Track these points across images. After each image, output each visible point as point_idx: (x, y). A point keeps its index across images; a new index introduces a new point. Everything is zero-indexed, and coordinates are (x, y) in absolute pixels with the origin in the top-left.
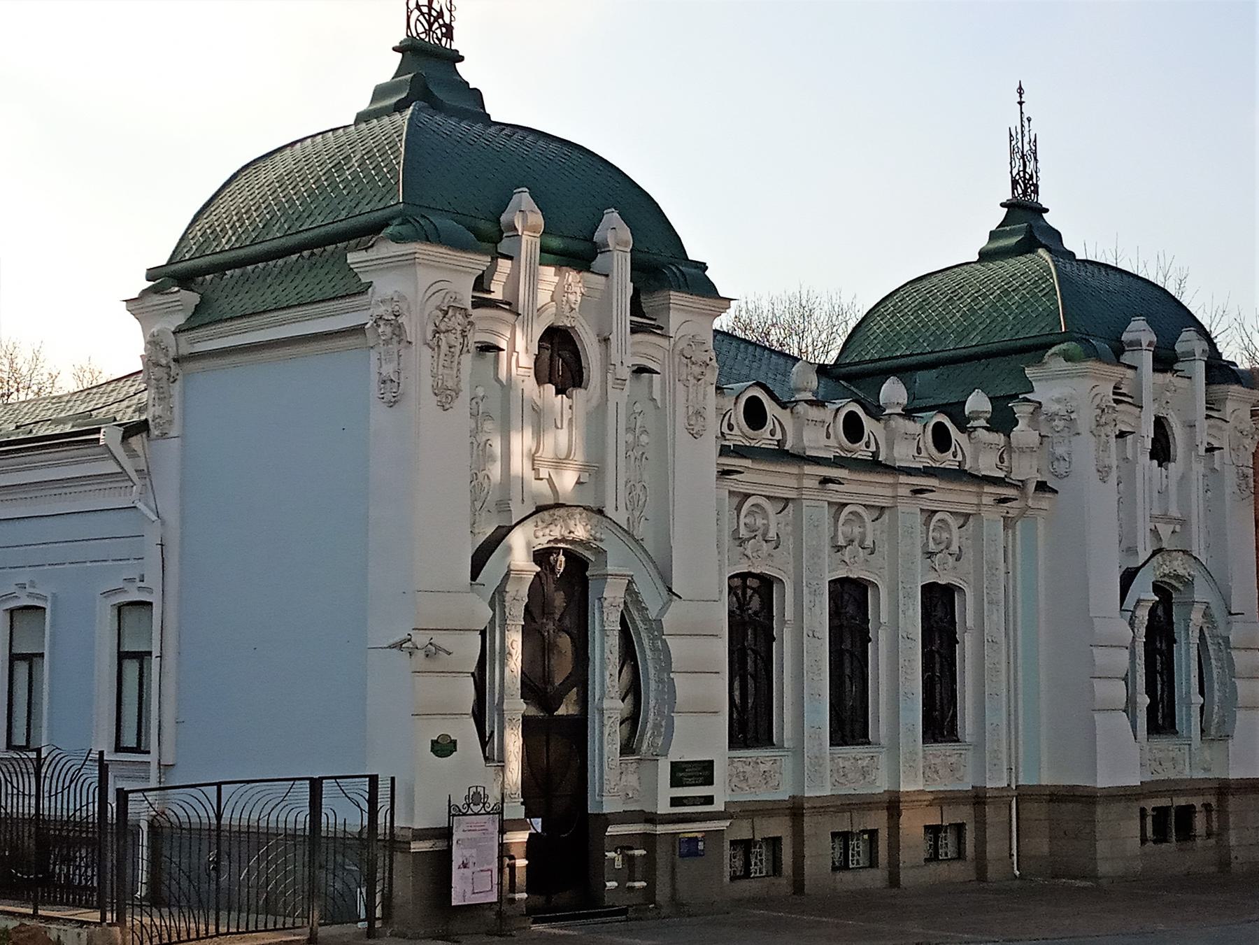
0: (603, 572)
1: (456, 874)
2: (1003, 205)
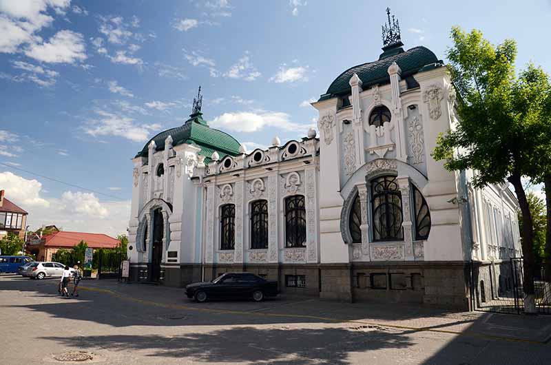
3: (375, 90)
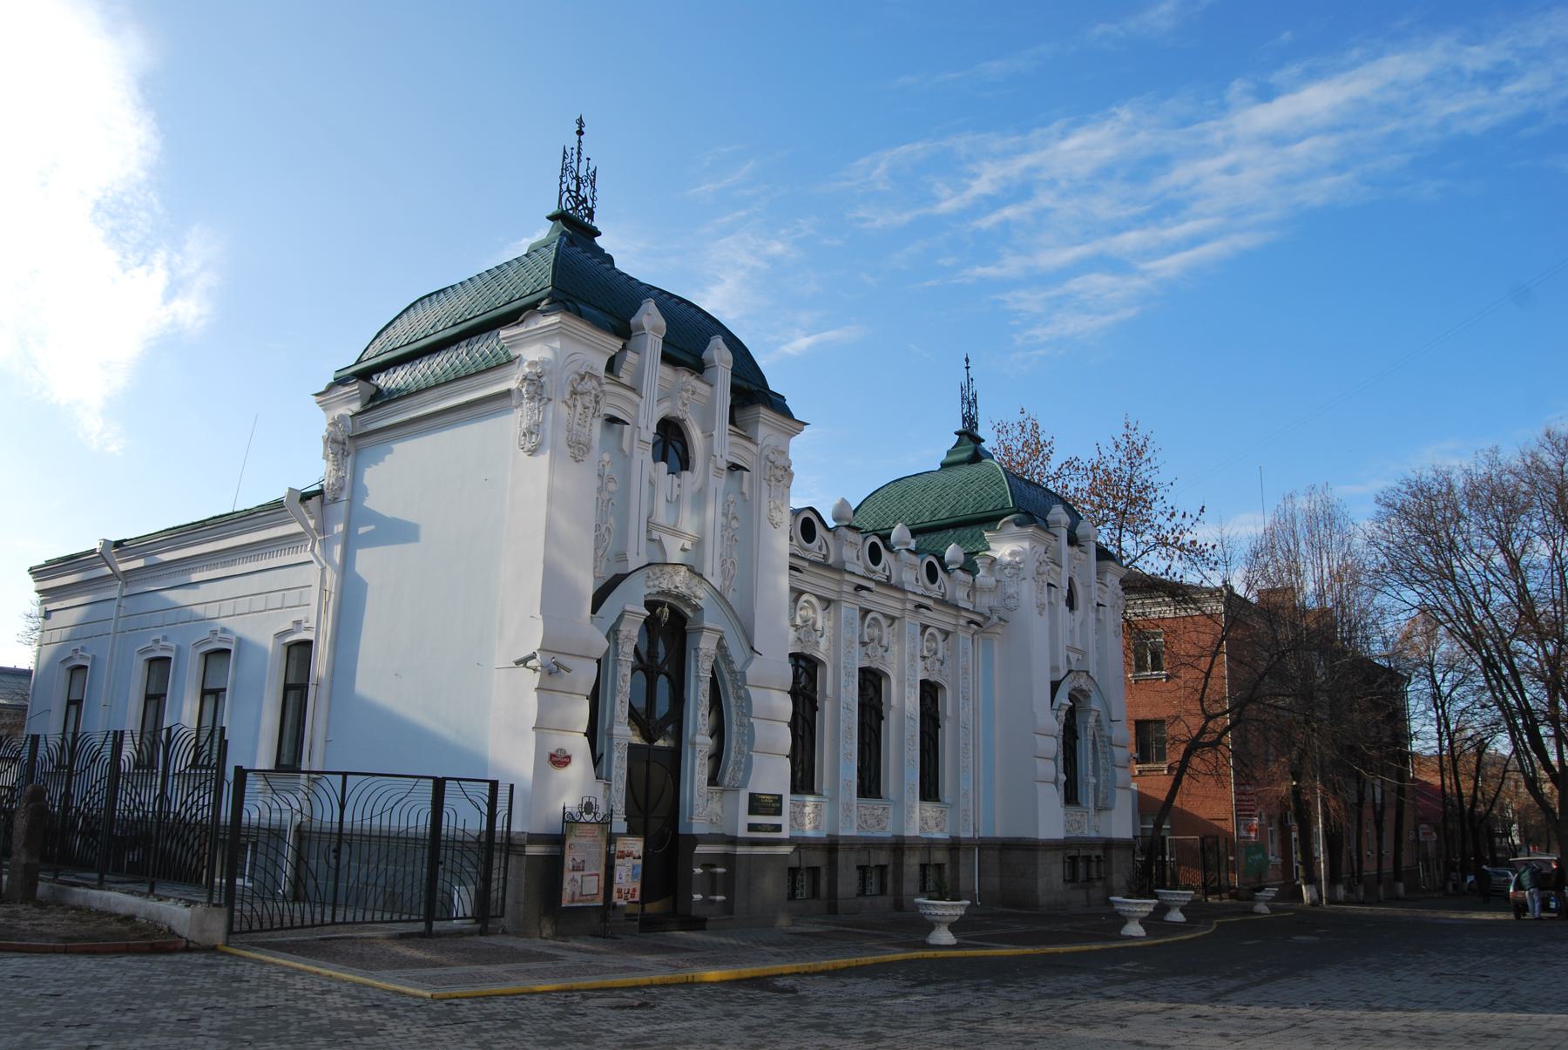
0: (701, 626)
1: (568, 876)
2: (956, 433)
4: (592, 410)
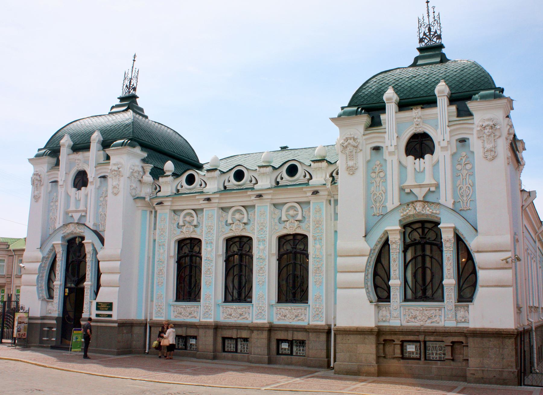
3: (416, 113)
4: (39, 184)
